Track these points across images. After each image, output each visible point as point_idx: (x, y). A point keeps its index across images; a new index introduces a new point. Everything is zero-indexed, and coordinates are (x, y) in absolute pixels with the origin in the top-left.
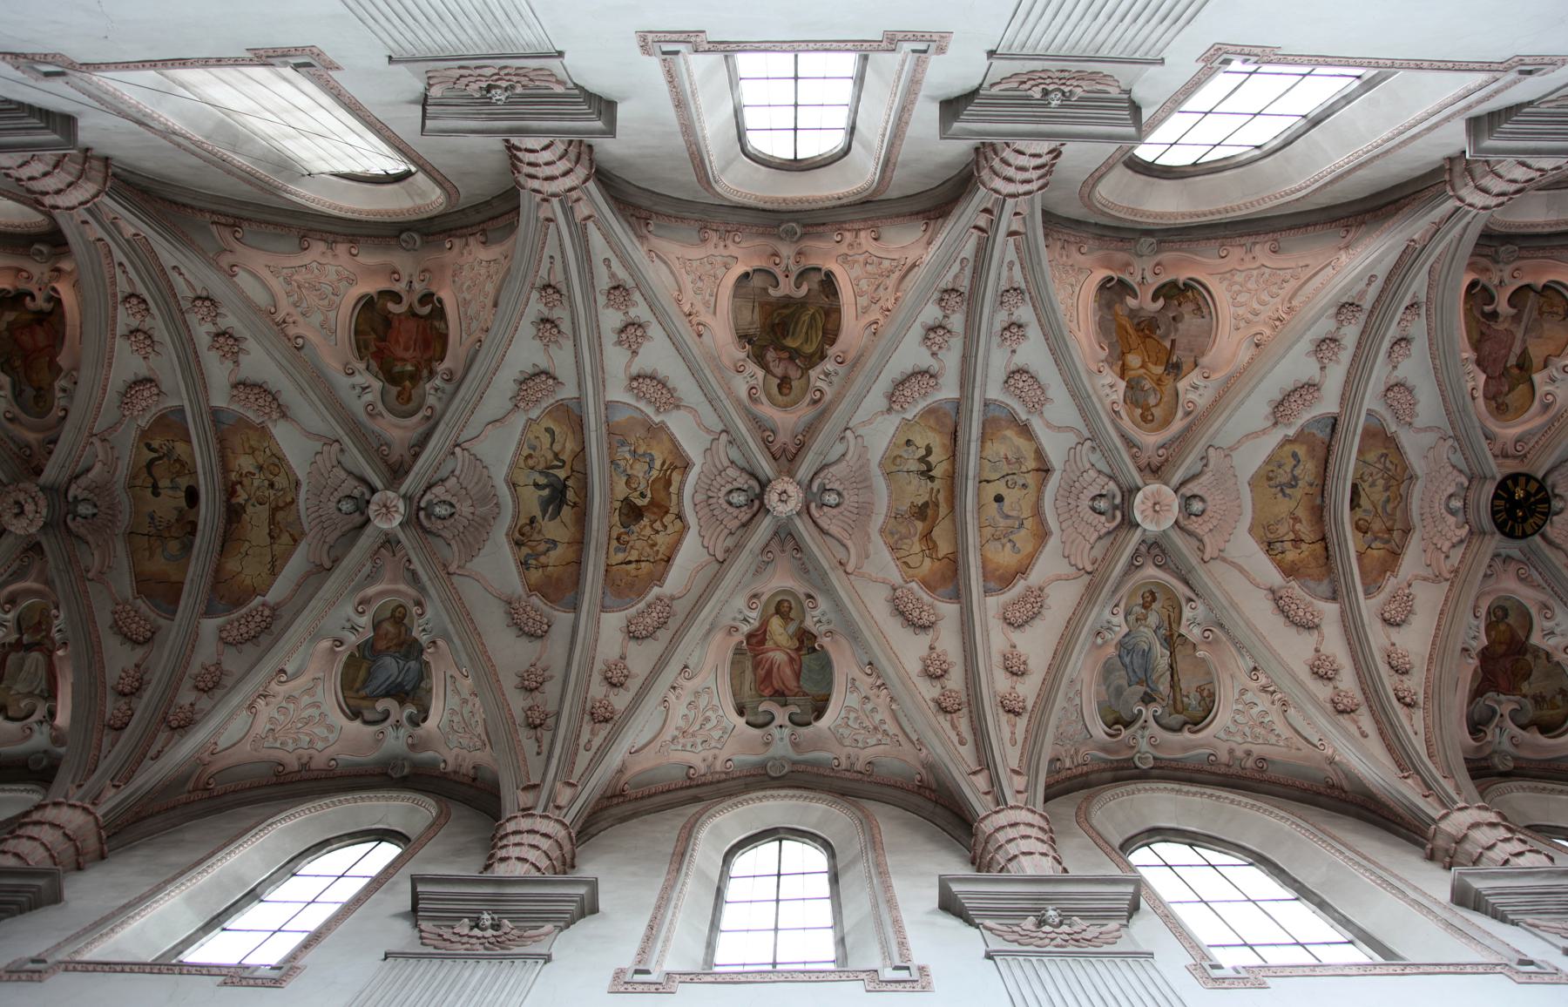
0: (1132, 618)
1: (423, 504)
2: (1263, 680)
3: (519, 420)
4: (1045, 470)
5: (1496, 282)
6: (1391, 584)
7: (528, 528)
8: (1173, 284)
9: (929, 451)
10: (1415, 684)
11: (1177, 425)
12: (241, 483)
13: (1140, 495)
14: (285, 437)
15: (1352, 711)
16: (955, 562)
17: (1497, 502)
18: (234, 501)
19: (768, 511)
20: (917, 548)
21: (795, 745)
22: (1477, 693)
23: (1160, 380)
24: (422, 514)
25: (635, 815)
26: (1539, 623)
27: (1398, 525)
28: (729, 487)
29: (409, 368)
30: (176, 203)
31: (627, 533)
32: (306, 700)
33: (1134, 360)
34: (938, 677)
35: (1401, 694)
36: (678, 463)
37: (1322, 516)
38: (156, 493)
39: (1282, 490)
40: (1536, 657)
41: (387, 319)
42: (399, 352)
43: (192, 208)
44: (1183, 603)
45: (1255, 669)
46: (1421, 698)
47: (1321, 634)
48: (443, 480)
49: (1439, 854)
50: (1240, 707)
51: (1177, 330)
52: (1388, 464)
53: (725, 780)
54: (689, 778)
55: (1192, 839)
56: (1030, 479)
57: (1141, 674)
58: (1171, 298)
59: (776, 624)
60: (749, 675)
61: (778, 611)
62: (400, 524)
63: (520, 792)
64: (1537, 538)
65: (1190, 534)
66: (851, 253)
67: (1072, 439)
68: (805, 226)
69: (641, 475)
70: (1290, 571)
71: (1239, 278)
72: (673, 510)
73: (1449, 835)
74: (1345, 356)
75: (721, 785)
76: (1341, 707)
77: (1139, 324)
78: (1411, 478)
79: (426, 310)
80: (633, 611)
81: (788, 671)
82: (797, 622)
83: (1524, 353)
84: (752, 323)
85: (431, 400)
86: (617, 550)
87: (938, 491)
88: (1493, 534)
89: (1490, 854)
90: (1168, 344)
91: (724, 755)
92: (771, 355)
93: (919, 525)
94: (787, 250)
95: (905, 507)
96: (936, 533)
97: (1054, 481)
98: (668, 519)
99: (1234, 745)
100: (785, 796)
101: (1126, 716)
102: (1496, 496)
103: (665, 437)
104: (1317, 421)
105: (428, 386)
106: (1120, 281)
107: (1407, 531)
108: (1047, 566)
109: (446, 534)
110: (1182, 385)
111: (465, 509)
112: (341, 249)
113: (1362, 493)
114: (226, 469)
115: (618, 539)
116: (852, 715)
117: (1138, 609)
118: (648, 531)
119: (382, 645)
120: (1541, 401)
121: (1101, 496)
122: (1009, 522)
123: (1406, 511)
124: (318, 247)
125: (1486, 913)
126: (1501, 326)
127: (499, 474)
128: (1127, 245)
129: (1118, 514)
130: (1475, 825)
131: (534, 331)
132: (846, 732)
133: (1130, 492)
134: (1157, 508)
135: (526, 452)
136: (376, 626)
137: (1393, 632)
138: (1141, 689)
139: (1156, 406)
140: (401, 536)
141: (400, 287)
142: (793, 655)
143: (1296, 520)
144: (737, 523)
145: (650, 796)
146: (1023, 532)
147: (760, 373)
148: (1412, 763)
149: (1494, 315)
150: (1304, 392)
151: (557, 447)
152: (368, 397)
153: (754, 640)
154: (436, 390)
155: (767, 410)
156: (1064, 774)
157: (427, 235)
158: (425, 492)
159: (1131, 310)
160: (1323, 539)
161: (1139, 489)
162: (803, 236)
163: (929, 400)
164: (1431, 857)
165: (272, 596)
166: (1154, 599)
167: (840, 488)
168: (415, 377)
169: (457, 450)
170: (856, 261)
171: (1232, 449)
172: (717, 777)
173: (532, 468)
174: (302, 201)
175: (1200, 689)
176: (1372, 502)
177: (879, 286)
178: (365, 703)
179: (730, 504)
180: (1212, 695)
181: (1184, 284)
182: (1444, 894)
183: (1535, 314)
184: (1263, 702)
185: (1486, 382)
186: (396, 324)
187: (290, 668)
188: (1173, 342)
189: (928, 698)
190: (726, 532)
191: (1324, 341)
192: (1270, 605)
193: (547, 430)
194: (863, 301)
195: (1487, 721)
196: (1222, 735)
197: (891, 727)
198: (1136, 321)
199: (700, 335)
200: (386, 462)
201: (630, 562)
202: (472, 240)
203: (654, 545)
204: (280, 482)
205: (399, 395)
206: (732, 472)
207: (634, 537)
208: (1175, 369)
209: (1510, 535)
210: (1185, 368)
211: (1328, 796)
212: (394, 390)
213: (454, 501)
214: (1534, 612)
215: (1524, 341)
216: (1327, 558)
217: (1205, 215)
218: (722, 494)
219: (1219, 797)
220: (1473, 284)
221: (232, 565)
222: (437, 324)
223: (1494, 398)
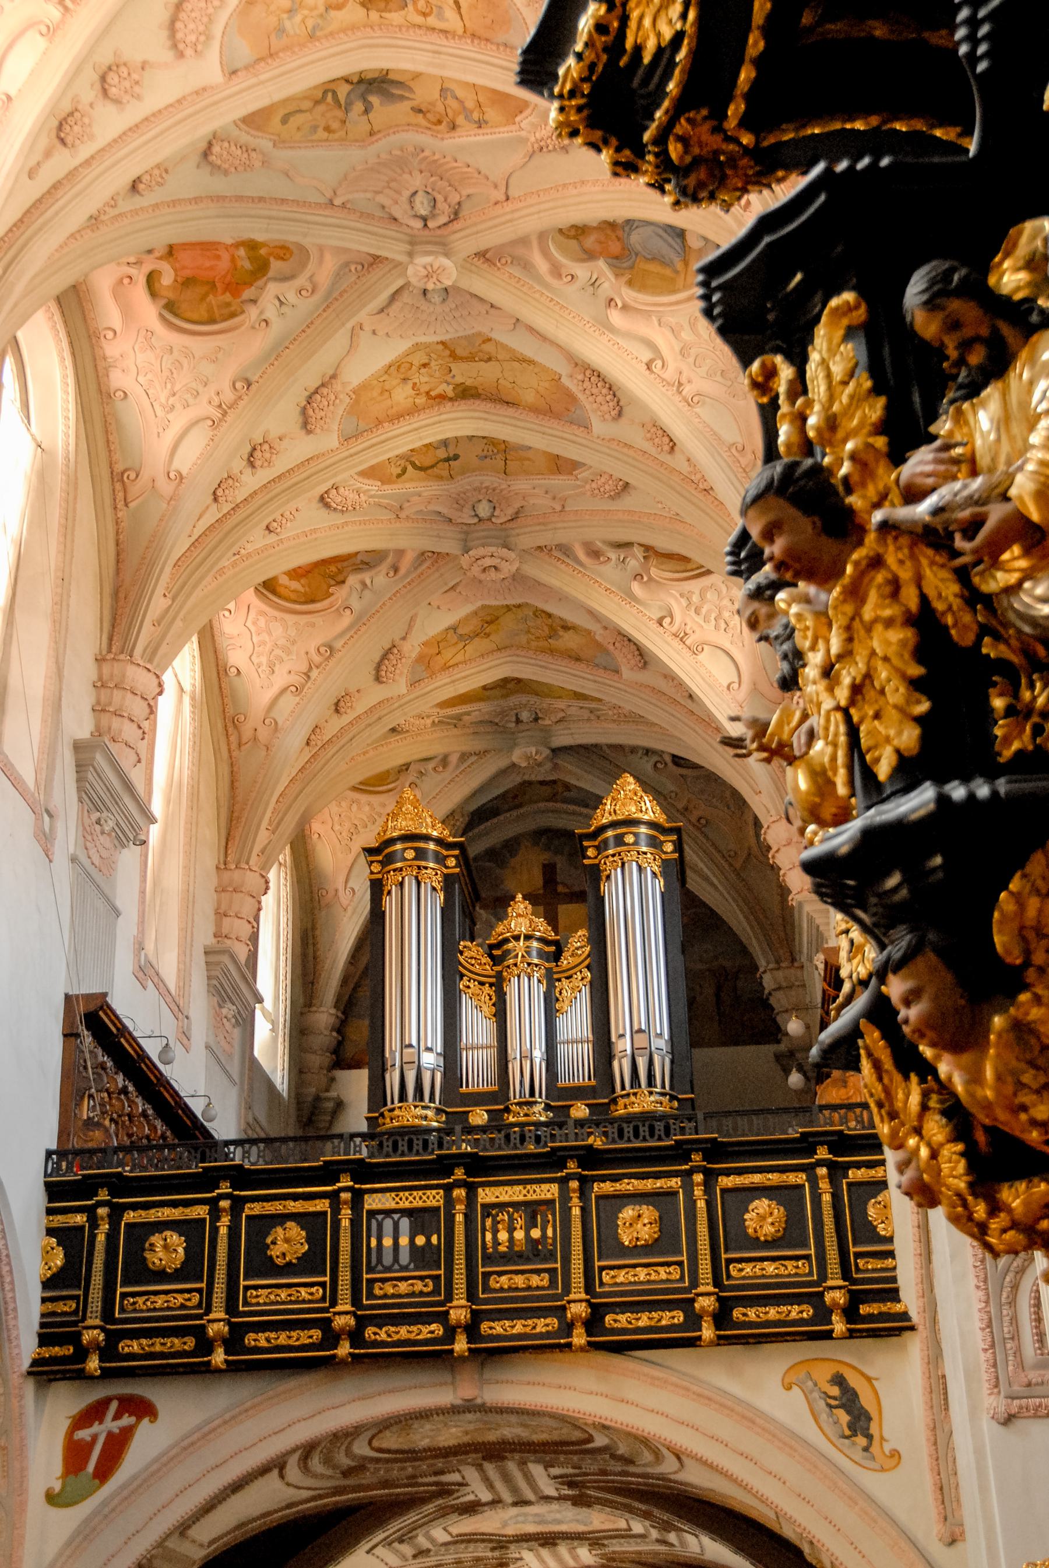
12: (427, 393)
18: (451, 394)
30: (118, 554)
38: (456, 457)
41: (187, 283)
43: (117, 533)
86: (441, 16)
112: (112, 349)
114: (414, 410)
119: (615, 248)
124: (118, 379)
135: (321, 134)
136: (590, 256)
152: (291, 297)
169: (337, 202)
174: (72, 432)
186: (188, 273)
204: (419, 358)
212: (275, 265)
213: (407, 194)
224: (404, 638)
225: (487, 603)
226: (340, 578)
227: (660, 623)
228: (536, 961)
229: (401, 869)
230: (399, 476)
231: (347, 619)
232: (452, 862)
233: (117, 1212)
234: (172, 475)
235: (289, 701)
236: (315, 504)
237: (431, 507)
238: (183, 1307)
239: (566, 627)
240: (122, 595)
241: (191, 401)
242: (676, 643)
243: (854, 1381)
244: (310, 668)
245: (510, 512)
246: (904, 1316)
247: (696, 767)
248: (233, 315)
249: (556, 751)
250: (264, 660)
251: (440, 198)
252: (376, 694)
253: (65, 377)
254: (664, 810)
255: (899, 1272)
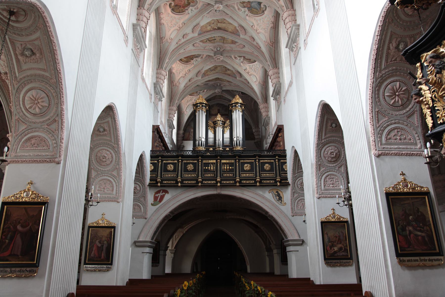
12: (213, 28)
14: (203, 23)
18: (217, 29)
30: (160, 52)
32: (259, 22)
38: (215, 39)
41: (176, 6)
42: (183, 3)
62: (222, 4)
112: (162, 16)
114: (210, 31)
119: (249, 6)
124: (162, 21)
136: (244, 7)
141: (168, 4)
152: (194, 9)
165: (236, 25)
178: (261, 10)
186: (176, 4)
187: (252, 25)
204: (212, 22)
205: (192, 2)
212: (191, 4)
221: (230, 30)
224: (202, 70)
225: (216, 65)
226: (192, 59)
227: (245, 70)
228: (221, 125)
229: (199, 108)
230: (206, 42)
231: (193, 66)
232: (207, 108)
233: (162, 161)
234: (170, 39)
235: (182, 79)
236: (192, 45)
237: (210, 48)
238: (173, 176)
239: (229, 70)
240: (161, 59)
241: (174, 26)
242: (247, 74)
243: (280, 192)
244: (186, 74)
245: (223, 49)
246: (288, 183)
247: (247, 95)
248: (183, 12)
249: (223, 91)
250: (178, 72)
252: (197, 79)
253: (154, 20)
254: (243, 101)
255: (288, 176)
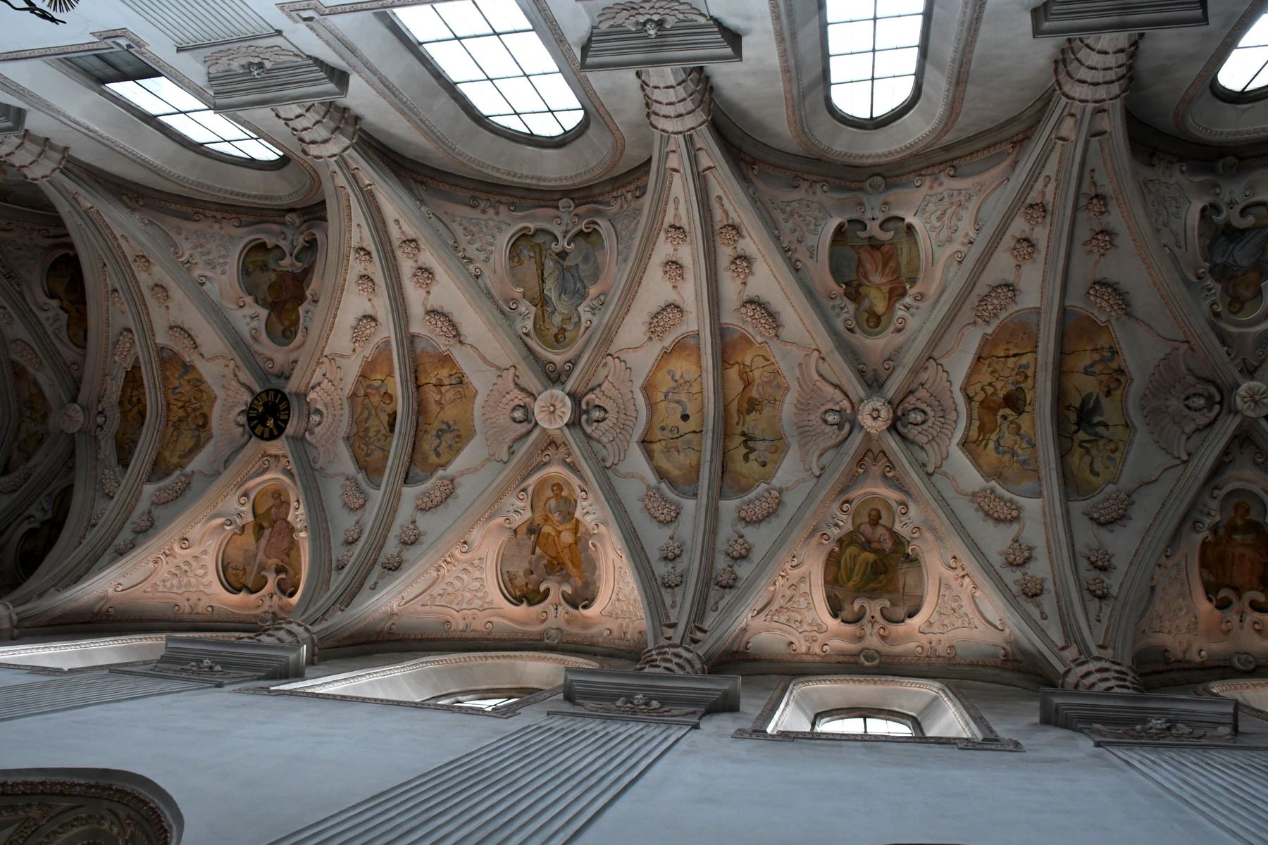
0: (575, 319)
1: (1217, 407)
2: (471, 268)
3: (1126, 481)
4: (645, 443)
5: (275, 597)
6: (368, 351)
7: (1113, 386)
8: (531, 604)
9: (746, 457)
10: (357, 267)
11: (532, 481)
13: (566, 420)
15: (404, 242)
16: (724, 361)
17: (285, 417)
19: (890, 403)
20: (757, 373)
21: (861, 204)
22: (308, 271)
23: (546, 521)
24: (1218, 398)
25: (1001, 127)
26: (261, 324)
27: (359, 400)
28: (925, 426)
29: (1238, 537)
31: (1018, 382)
33: (567, 538)
34: (739, 257)
35: (367, 257)
36: (973, 446)
37: (419, 406)
39: (449, 426)
40: (264, 300)
44: (532, 333)
45: (477, 277)
46: (352, 255)
47: (424, 305)
48: (1198, 430)
49: (351, 121)
50: (490, 248)
51: (530, 563)
52: (365, 448)
53: (922, 169)
54: (953, 167)
55: (530, 139)
56: (658, 435)
57: (568, 275)
58: (534, 591)
59: (880, 307)
60: (903, 260)
61: (879, 318)
62: (1238, 386)
63: (1108, 129)
64: (258, 390)
65: (523, 390)
66: (815, 633)
67: (622, 468)
68: (856, 663)
69: (1007, 435)
70: (446, 360)
71: (478, 603)
72: (975, 405)
73: (344, 135)
74: (395, 531)
75: (926, 164)
76: (413, 245)
77: (562, 569)
78: (348, 438)
79: (1223, 593)
80: (1013, 309)
81: (868, 266)
82: (862, 308)
83: (258, 539)
84: (904, 574)
85: (1214, 505)
86: (1027, 367)
87: (738, 424)
88: (290, 393)
89: (318, 118)
90: (538, 551)
91: (924, 190)
92: (888, 545)
93: (754, 393)
94: (873, 642)
95: (767, 410)
96: (740, 387)
97: (638, 434)
98: (981, 396)
99: (495, 217)
100: (868, 157)
101: (580, 240)
102: (286, 422)
103: (986, 468)
104: (421, 481)
105: (1218, 518)
106: (577, 608)
107: (354, 395)
108: (644, 360)
109: (1190, 379)
110: (528, 514)
111: (1175, 404)
113: (386, 426)
115: (1026, 377)
116: (812, 227)
117: (569, 327)
118: (999, 385)
120: (248, 498)
121: (598, 421)
122: (676, 397)
123: (353, 412)
125: (327, 65)
126: (273, 562)
127: (1142, 435)
128: (569, 639)
129: (584, 407)
130: (325, 141)
131: (1114, 561)
132: (816, 214)
133: (574, 424)
134: (552, 409)
135: (1118, 455)
137: (370, 312)
138: (568, 263)
139: (549, 499)
140: (1238, 376)
142: (864, 281)
143: (439, 403)
144: (918, 394)
145: (988, 147)
146: (664, 390)
147: (898, 527)
148: (364, 197)
149: (279, 570)
150: (429, 505)
151: (1087, 459)
153: (900, 291)
154: (1209, 514)
155: (892, 495)
156: (632, 187)
157: (1226, 667)
158: (1215, 419)
159: (568, 582)
160: (418, 387)
161: (567, 425)
162: (857, 655)
163: (746, 498)
164: (357, 119)
166: (556, 336)
167: (824, 426)
168: (1232, 528)
169: (1185, 457)
170: (810, 624)
171: (489, 460)
172: (929, 171)
173: (1111, 441)
175: (520, 263)
176: (379, 419)
177: (790, 600)
179: (924, 412)
180: (511, 258)
181: (522, 602)
182: (354, 80)
183: (248, 569)
184: (471, 251)
185: (287, 515)
188: (533, 553)
189: (748, 239)
190: (926, 386)
191: (413, 543)
192: (464, 330)
193: (1097, 474)
194: (804, 588)
195: (304, 249)
196: (504, 227)
197: (780, 217)
198: (564, 572)
199: (954, 558)
200: (1258, 447)
201: (1015, 355)
202: (1180, 655)
203: (993, 372)
205: (1248, 511)
206: (923, 439)
207: (1011, 379)
208: (533, 529)
209: (278, 392)
210: (524, 529)
211: (425, 176)
212: (1253, 516)
213: (1186, 411)
214: (264, 335)
215: (257, 548)
216: (416, 371)
217: (503, 656)
218: (932, 420)
219: (508, 174)
220: (292, 595)
222: (1212, 579)
223: (282, 503)
251: (1192, 391)
